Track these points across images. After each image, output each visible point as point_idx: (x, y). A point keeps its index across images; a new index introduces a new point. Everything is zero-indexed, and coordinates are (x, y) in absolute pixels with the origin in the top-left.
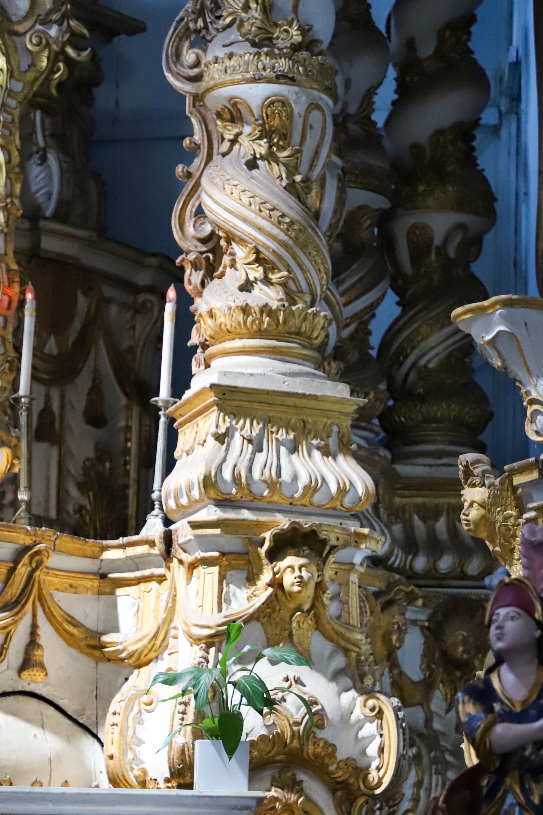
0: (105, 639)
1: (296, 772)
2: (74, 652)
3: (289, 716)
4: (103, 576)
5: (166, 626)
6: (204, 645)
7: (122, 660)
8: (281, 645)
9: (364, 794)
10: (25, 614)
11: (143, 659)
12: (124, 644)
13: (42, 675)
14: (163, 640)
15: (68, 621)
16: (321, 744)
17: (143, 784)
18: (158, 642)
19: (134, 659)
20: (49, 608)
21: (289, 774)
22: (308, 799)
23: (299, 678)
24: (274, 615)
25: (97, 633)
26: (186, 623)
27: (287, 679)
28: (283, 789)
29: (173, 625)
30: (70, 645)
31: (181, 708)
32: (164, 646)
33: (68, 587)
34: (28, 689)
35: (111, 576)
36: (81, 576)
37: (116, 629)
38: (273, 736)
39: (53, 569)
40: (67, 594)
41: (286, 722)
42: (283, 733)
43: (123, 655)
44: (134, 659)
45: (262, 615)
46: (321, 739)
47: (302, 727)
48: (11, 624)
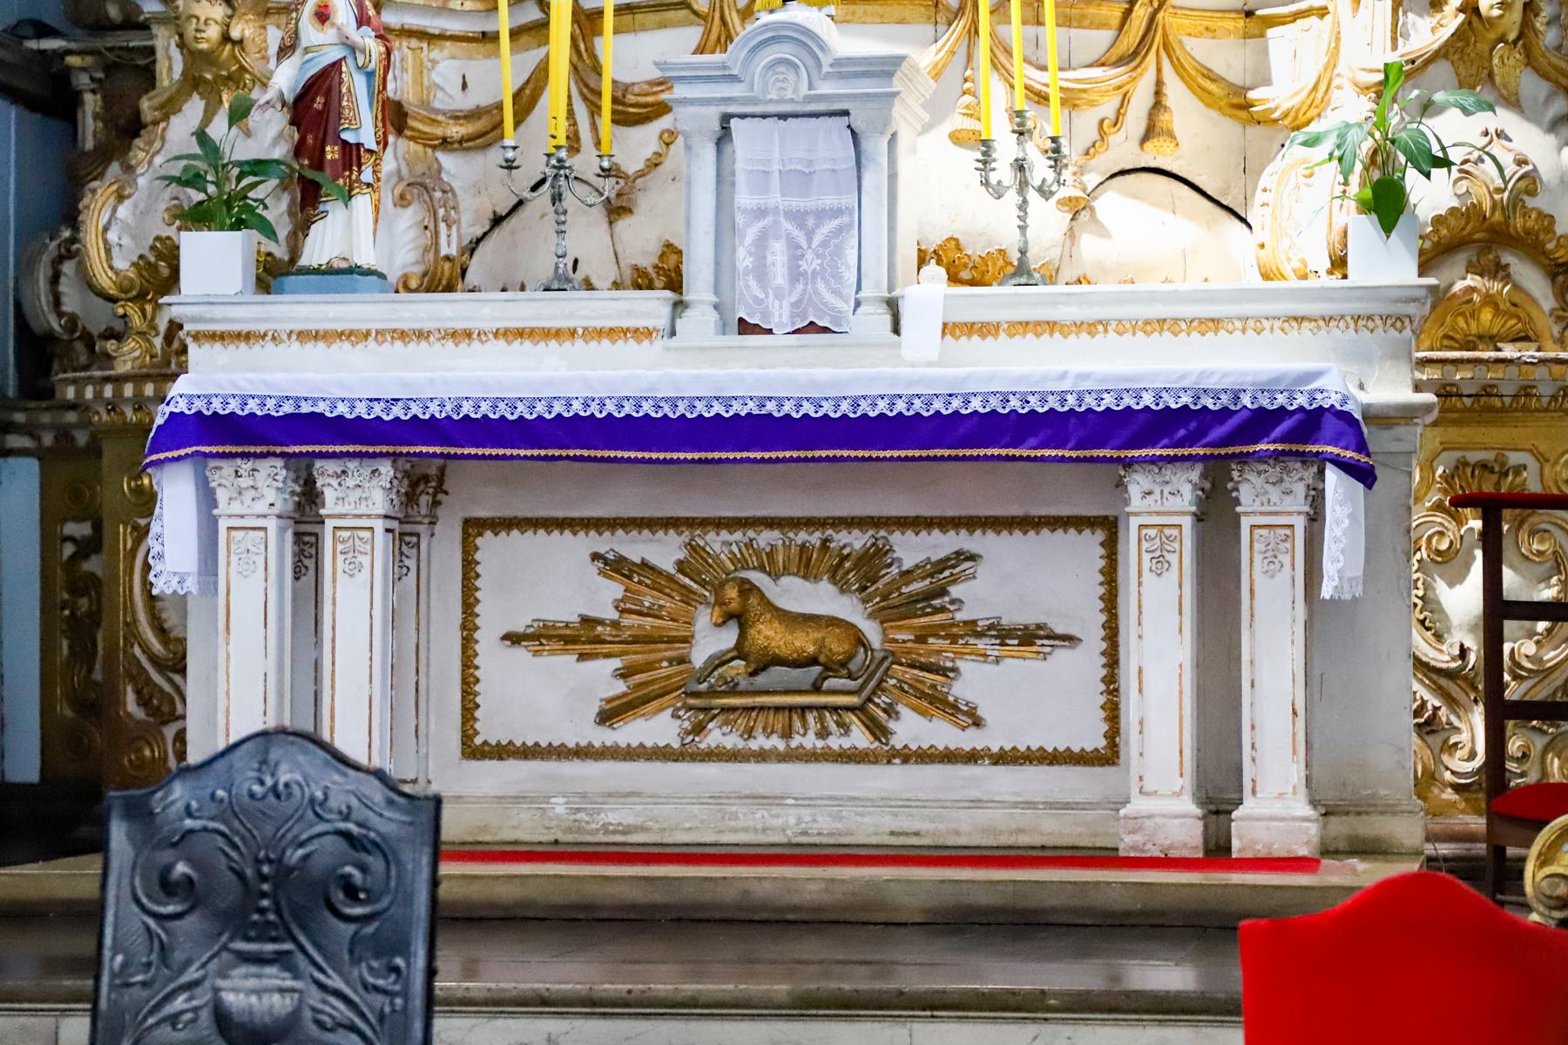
0: (1251, 95)
1: (1500, 253)
2: (1214, 114)
3: (1488, 182)
4: (1249, 14)
5: (1328, 74)
6: (1373, 95)
7: (1276, 121)
8: (1478, 88)
10: (1146, 69)
11: (1301, 119)
12: (1277, 101)
13: (1172, 146)
14: (1326, 92)
15: (1203, 75)
16: (1534, 216)
17: (1304, 277)
18: (1320, 95)
19: (1290, 119)
20: (1178, 59)
21: (1491, 257)
22: (1517, 287)
23: (1502, 131)
24: (1468, 51)
25: (1243, 88)
26: (1350, 68)
27: (1486, 134)
28: (1482, 275)
29: (1336, 72)
30: (1207, 105)
32: (1325, 101)
33: (1204, 31)
34: (1153, 164)
35: (1258, 13)
36: (1219, 15)
37: (1267, 82)
38: (1467, 208)
39: (1181, 8)
40: (1202, 41)
41: (1484, 189)
42: (1480, 203)
43: (1275, 116)
44: (1290, 119)
45: (1452, 50)
46: (1533, 209)
47: (1506, 195)
48: (1128, 83)
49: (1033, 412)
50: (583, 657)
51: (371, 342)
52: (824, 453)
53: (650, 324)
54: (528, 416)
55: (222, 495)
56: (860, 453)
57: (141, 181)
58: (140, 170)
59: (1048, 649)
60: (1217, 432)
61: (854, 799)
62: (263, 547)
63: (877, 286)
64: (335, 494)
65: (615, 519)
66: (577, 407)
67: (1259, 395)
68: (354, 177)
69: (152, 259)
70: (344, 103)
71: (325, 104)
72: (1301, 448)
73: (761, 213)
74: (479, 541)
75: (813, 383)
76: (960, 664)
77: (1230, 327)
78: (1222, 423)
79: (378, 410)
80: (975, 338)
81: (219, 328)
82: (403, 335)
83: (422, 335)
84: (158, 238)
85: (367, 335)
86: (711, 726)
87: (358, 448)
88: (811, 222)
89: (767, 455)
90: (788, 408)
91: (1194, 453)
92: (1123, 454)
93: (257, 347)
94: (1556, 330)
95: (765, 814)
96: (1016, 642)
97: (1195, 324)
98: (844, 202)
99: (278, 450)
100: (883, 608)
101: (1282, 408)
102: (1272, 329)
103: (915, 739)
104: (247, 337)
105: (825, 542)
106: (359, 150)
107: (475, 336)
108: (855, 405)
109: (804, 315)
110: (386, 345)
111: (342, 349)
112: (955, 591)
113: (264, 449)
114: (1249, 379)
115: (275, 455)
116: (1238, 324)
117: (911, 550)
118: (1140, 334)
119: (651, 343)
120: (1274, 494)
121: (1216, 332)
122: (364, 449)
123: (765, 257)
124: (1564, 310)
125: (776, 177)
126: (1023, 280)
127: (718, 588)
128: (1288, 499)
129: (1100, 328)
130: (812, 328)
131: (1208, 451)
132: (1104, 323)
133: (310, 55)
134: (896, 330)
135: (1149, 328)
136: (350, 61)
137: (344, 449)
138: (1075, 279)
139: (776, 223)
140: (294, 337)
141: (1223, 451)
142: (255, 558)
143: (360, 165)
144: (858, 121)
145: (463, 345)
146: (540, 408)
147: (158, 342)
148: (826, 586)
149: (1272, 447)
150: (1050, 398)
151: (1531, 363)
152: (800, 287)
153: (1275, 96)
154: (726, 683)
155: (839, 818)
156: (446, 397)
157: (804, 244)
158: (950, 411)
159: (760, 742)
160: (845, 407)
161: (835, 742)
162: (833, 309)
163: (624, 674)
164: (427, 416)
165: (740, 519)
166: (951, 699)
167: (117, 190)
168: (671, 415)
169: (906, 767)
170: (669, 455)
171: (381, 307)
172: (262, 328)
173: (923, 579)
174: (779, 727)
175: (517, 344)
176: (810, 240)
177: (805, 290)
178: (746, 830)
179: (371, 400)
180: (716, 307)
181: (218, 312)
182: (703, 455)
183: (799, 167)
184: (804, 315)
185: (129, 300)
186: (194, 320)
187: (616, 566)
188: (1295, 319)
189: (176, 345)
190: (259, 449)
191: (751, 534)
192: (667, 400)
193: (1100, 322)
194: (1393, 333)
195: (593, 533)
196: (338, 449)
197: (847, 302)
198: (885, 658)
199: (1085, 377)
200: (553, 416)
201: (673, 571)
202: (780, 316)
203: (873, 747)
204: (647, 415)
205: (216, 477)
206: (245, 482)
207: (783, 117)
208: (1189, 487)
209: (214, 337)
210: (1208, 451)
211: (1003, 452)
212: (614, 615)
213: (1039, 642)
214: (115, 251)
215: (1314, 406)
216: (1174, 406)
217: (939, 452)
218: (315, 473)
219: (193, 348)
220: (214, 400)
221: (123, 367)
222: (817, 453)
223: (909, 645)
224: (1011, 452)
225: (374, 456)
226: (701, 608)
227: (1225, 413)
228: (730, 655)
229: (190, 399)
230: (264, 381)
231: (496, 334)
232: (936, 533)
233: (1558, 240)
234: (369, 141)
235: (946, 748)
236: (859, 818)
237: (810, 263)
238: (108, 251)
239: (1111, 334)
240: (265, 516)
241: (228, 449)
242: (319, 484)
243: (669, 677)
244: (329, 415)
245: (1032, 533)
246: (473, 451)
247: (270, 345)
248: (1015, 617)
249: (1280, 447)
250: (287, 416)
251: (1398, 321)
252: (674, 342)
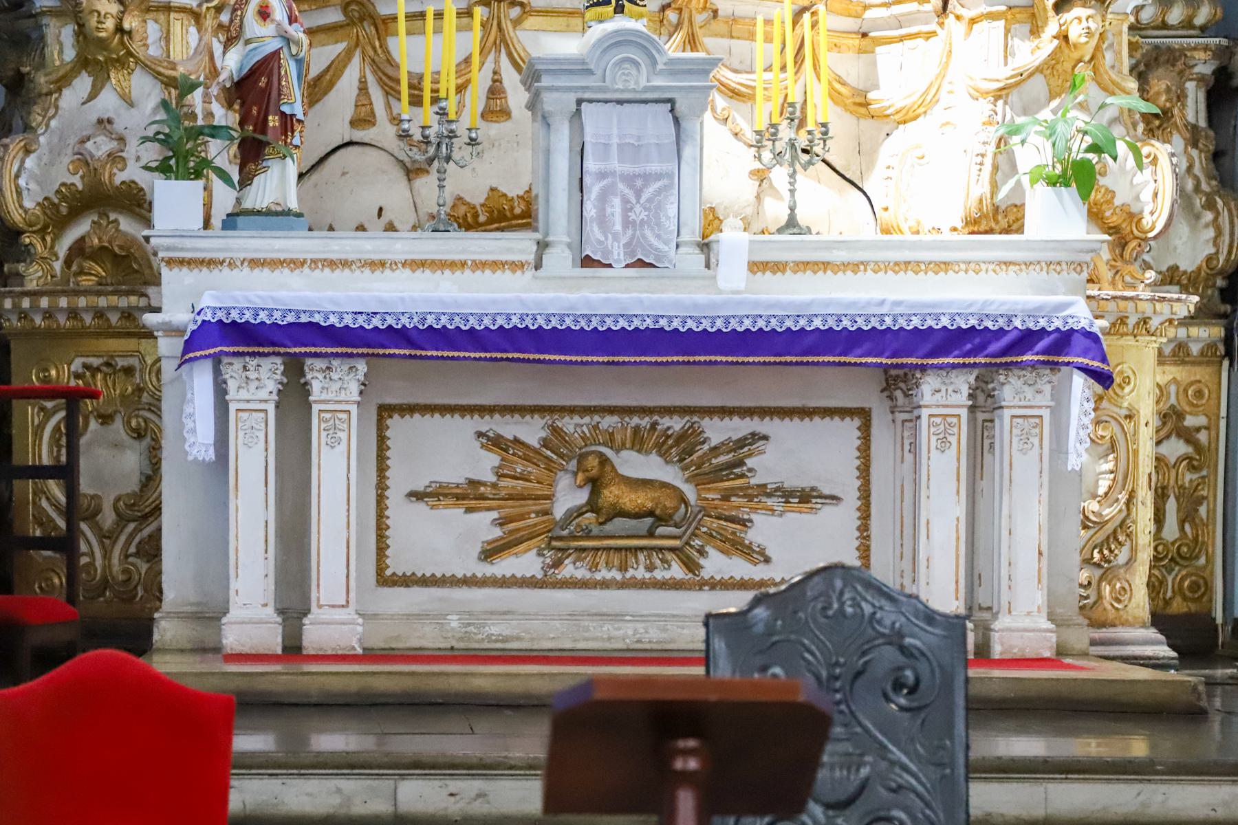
2: (839, 110)
7: (889, 116)
9: (1137, 238)
11: (911, 114)
16: (1103, 190)
17: (918, 232)
18: (929, 98)
31: (979, 159)
32: (935, 101)
36: (844, 35)
43: (889, 112)
44: (901, 115)
49: (859, 329)
50: (469, 510)
51: (306, 269)
52: (702, 358)
53: (523, 258)
54: (478, 328)
55: (232, 385)
56: (730, 359)
57: (42, 139)
58: (40, 131)
59: (819, 506)
60: (995, 347)
61: (674, 616)
62: (263, 425)
63: (693, 233)
64: (321, 385)
65: (494, 406)
66: (515, 321)
67: (1026, 319)
68: (289, 141)
69: (56, 201)
70: (284, 83)
71: (267, 83)
72: (1056, 359)
73: (602, 175)
74: (389, 422)
75: (696, 306)
76: (753, 516)
77: (957, 268)
78: (998, 339)
79: (361, 321)
80: (768, 273)
81: (188, 255)
82: (332, 264)
83: (346, 264)
84: (63, 184)
85: (303, 263)
86: (566, 562)
87: (344, 350)
88: (639, 183)
89: (659, 359)
90: (676, 324)
91: (977, 361)
92: (925, 361)
93: (216, 271)
94: (1110, 275)
95: (610, 627)
96: (797, 500)
97: (932, 266)
98: (664, 168)
99: (282, 350)
100: (697, 475)
101: (1043, 329)
102: (987, 271)
103: (719, 572)
104: (210, 263)
105: (654, 426)
106: (292, 120)
107: (388, 265)
108: (727, 322)
109: (633, 253)
110: (317, 271)
111: (284, 274)
112: (750, 462)
113: (270, 349)
114: (1020, 307)
115: (278, 354)
116: (963, 266)
117: (717, 431)
118: (890, 272)
119: (523, 273)
120: (1029, 392)
121: (946, 271)
122: (349, 350)
123: (604, 209)
124: (1115, 260)
125: (614, 149)
126: (795, 231)
127: (582, 458)
128: (1039, 396)
129: (862, 267)
130: (641, 264)
131: (988, 360)
132: (865, 264)
133: (254, 45)
134: (708, 266)
135: (897, 268)
136: (285, 50)
137: (334, 350)
138: (760, 230)
139: (614, 184)
140: (246, 264)
141: (998, 360)
142: (258, 433)
143: (293, 132)
144: (681, 107)
145: (378, 273)
146: (487, 322)
147: (58, 266)
148: (654, 458)
149: (1036, 358)
150: (872, 319)
151: (1107, 299)
152: (630, 232)
153: (887, 96)
154: (583, 530)
155: (665, 630)
156: (414, 311)
157: (634, 200)
158: (797, 328)
159: (604, 574)
160: (719, 324)
161: (659, 574)
162: (656, 249)
163: (501, 522)
164: (400, 326)
165: (590, 407)
166: (747, 542)
167: (25, 145)
168: (586, 328)
169: (713, 592)
170: (585, 359)
171: (316, 242)
172: (221, 256)
173: (728, 453)
174: (616, 562)
175: (419, 272)
176: (638, 197)
177: (633, 235)
178: (595, 639)
179: (355, 313)
180: (569, 246)
181: (188, 243)
182: (611, 359)
183: (632, 141)
184: (633, 253)
185: (34, 232)
186: (168, 249)
187: (495, 442)
188: (1005, 263)
189: (74, 268)
190: (266, 350)
191: (597, 418)
192: (584, 316)
193: (862, 263)
194: (1074, 275)
195: (476, 417)
196: (329, 350)
197: (666, 243)
198: (700, 511)
199: (898, 303)
200: (496, 327)
201: (537, 446)
202: (619, 254)
203: (687, 577)
204: (569, 328)
205: (229, 371)
206: (253, 375)
207: (620, 102)
208: (967, 386)
209: (182, 262)
210: (988, 360)
211: (837, 359)
212: (493, 479)
213: (814, 501)
214: (25, 193)
215: (1067, 328)
216: (964, 327)
217: (789, 359)
218: (306, 368)
219: (165, 272)
220: (232, 311)
221: (31, 285)
222: (697, 358)
223: (716, 502)
224: (843, 359)
225: (350, 356)
226: (560, 474)
227: (1001, 332)
228: (584, 509)
229: (214, 310)
230: (273, 299)
231: (404, 264)
232: (736, 419)
233: (1115, 210)
234: (298, 111)
235: (742, 579)
236: (679, 630)
237: (639, 214)
238: (19, 193)
239: (869, 272)
240: (266, 401)
241: (241, 349)
242: (309, 377)
243: (535, 525)
244: (323, 324)
245: (828, 419)
246: (435, 353)
247: (226, 270)
248: (794, 482)
249: (1042, 358)
250: (290, 325)
251: (1079, 266)
252: (540, 273)
